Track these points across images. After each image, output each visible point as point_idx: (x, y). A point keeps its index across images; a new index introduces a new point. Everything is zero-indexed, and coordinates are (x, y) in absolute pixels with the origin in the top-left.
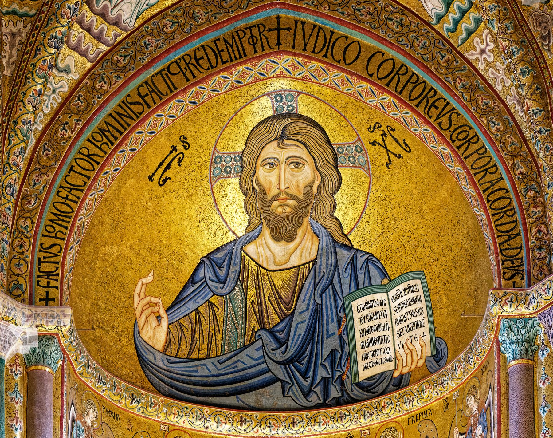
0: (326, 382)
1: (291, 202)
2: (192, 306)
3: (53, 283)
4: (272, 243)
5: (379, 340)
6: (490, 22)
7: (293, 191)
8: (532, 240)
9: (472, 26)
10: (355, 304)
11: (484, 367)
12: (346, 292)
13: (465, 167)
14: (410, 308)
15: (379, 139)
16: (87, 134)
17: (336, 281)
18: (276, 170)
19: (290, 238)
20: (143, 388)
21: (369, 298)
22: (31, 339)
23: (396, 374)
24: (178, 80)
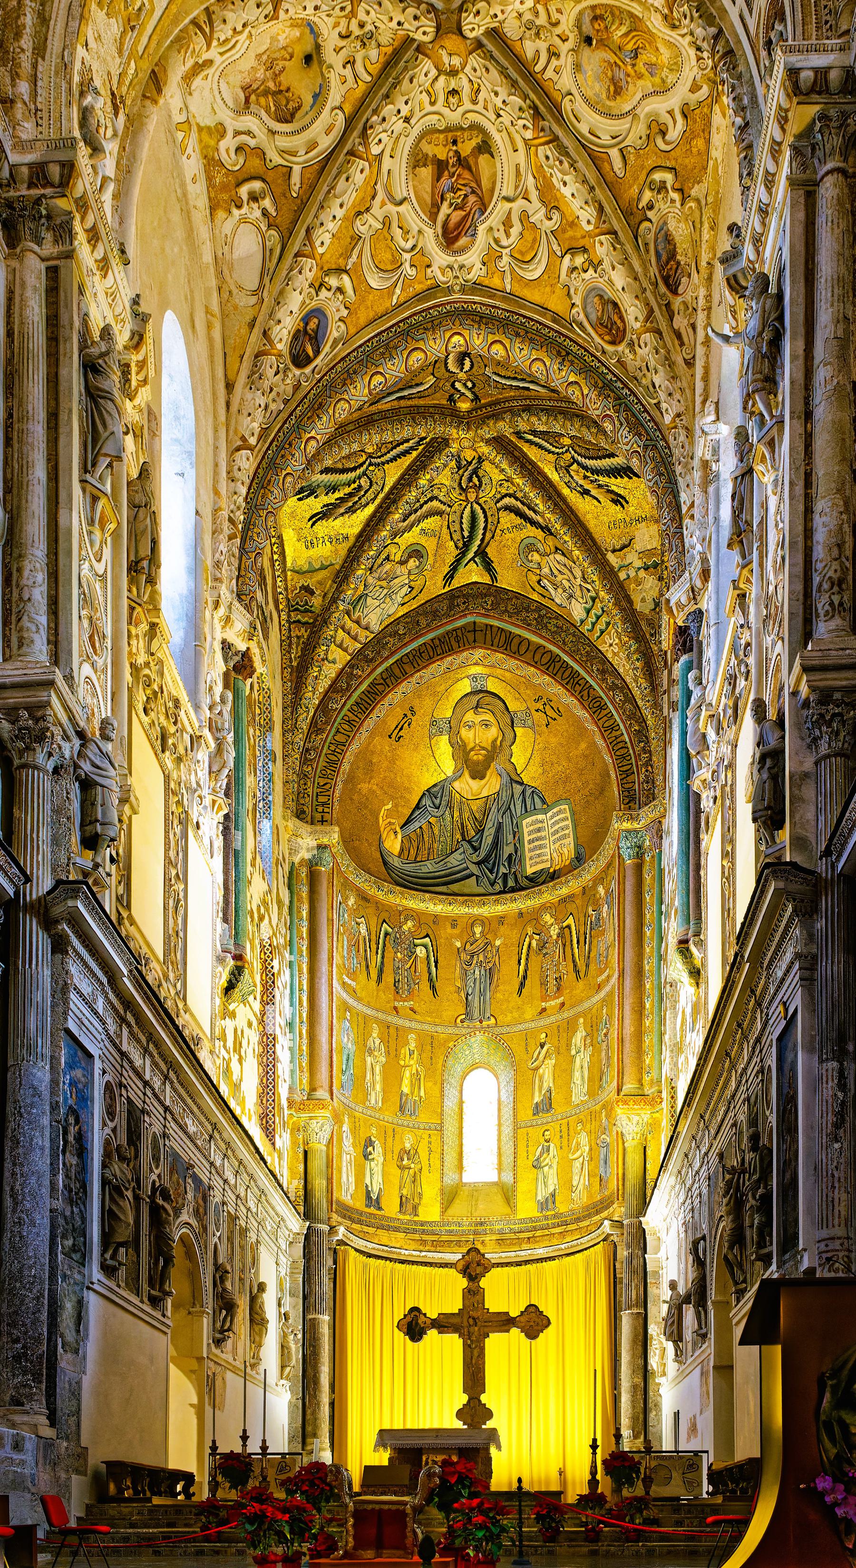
0: (505, 876)
1: (483, 752)
2: (417, 825)
3: (326, 810)
4: (470, 781)
5: (540, 847)
6: (616, 623)
7: (483, 745)
8: (642, 777)
9: (604, 627)
10: (524, 822)
11: (609, 865)
12: (519, 814)
13: (598, 727)
14: (562, 824)
15: (541, 707)
16: (348, 706)
17: (512, 807)
18: (473, 730)
19: (482, 777)
20: (385, 881)
21: (534, 818)
22: (312, 848)
23: (552, 870)
24: (407, 668)
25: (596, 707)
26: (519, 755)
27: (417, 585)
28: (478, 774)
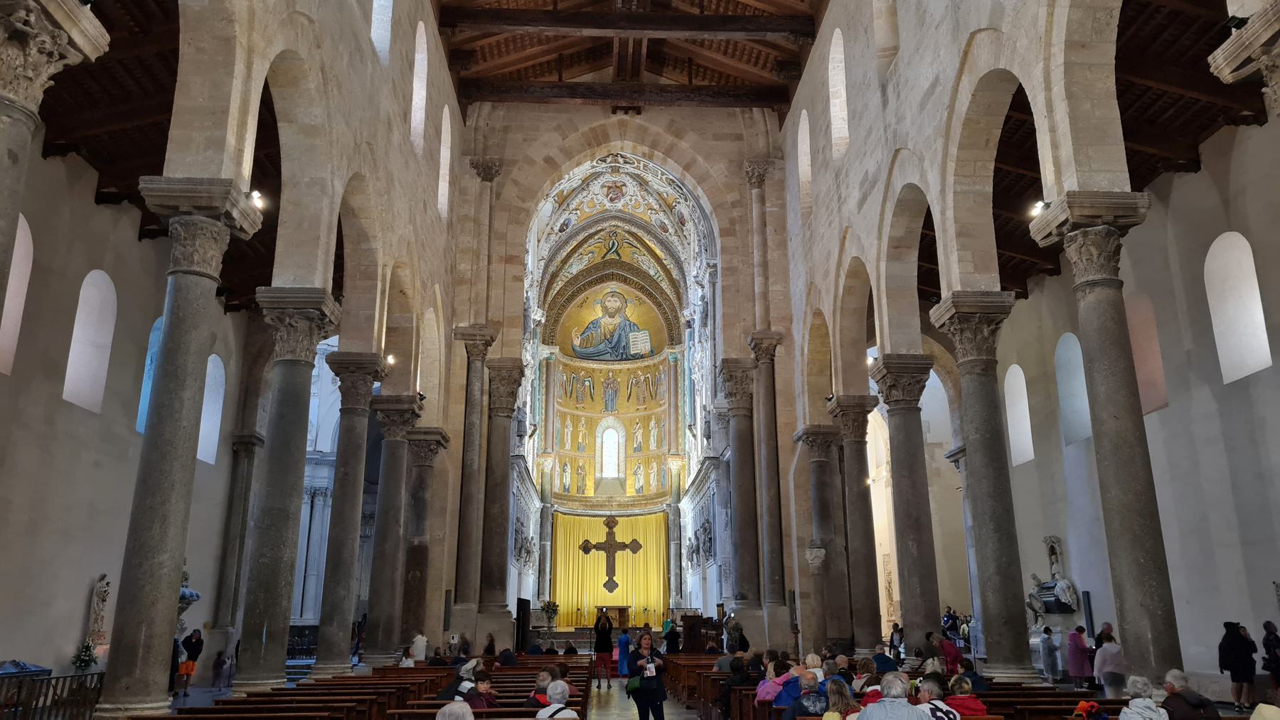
25: (659, 305)
26: (629, 312)
27: (591, 261)
28: (612, 316)
